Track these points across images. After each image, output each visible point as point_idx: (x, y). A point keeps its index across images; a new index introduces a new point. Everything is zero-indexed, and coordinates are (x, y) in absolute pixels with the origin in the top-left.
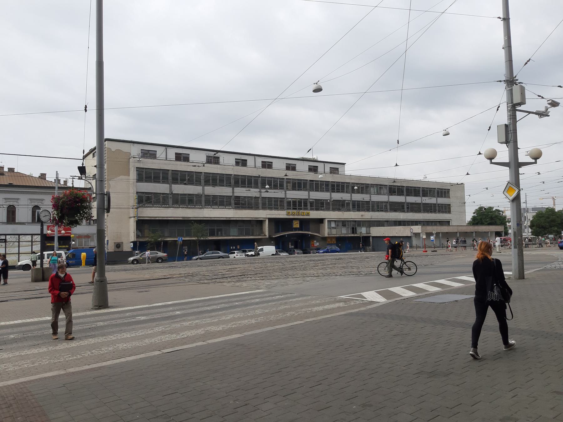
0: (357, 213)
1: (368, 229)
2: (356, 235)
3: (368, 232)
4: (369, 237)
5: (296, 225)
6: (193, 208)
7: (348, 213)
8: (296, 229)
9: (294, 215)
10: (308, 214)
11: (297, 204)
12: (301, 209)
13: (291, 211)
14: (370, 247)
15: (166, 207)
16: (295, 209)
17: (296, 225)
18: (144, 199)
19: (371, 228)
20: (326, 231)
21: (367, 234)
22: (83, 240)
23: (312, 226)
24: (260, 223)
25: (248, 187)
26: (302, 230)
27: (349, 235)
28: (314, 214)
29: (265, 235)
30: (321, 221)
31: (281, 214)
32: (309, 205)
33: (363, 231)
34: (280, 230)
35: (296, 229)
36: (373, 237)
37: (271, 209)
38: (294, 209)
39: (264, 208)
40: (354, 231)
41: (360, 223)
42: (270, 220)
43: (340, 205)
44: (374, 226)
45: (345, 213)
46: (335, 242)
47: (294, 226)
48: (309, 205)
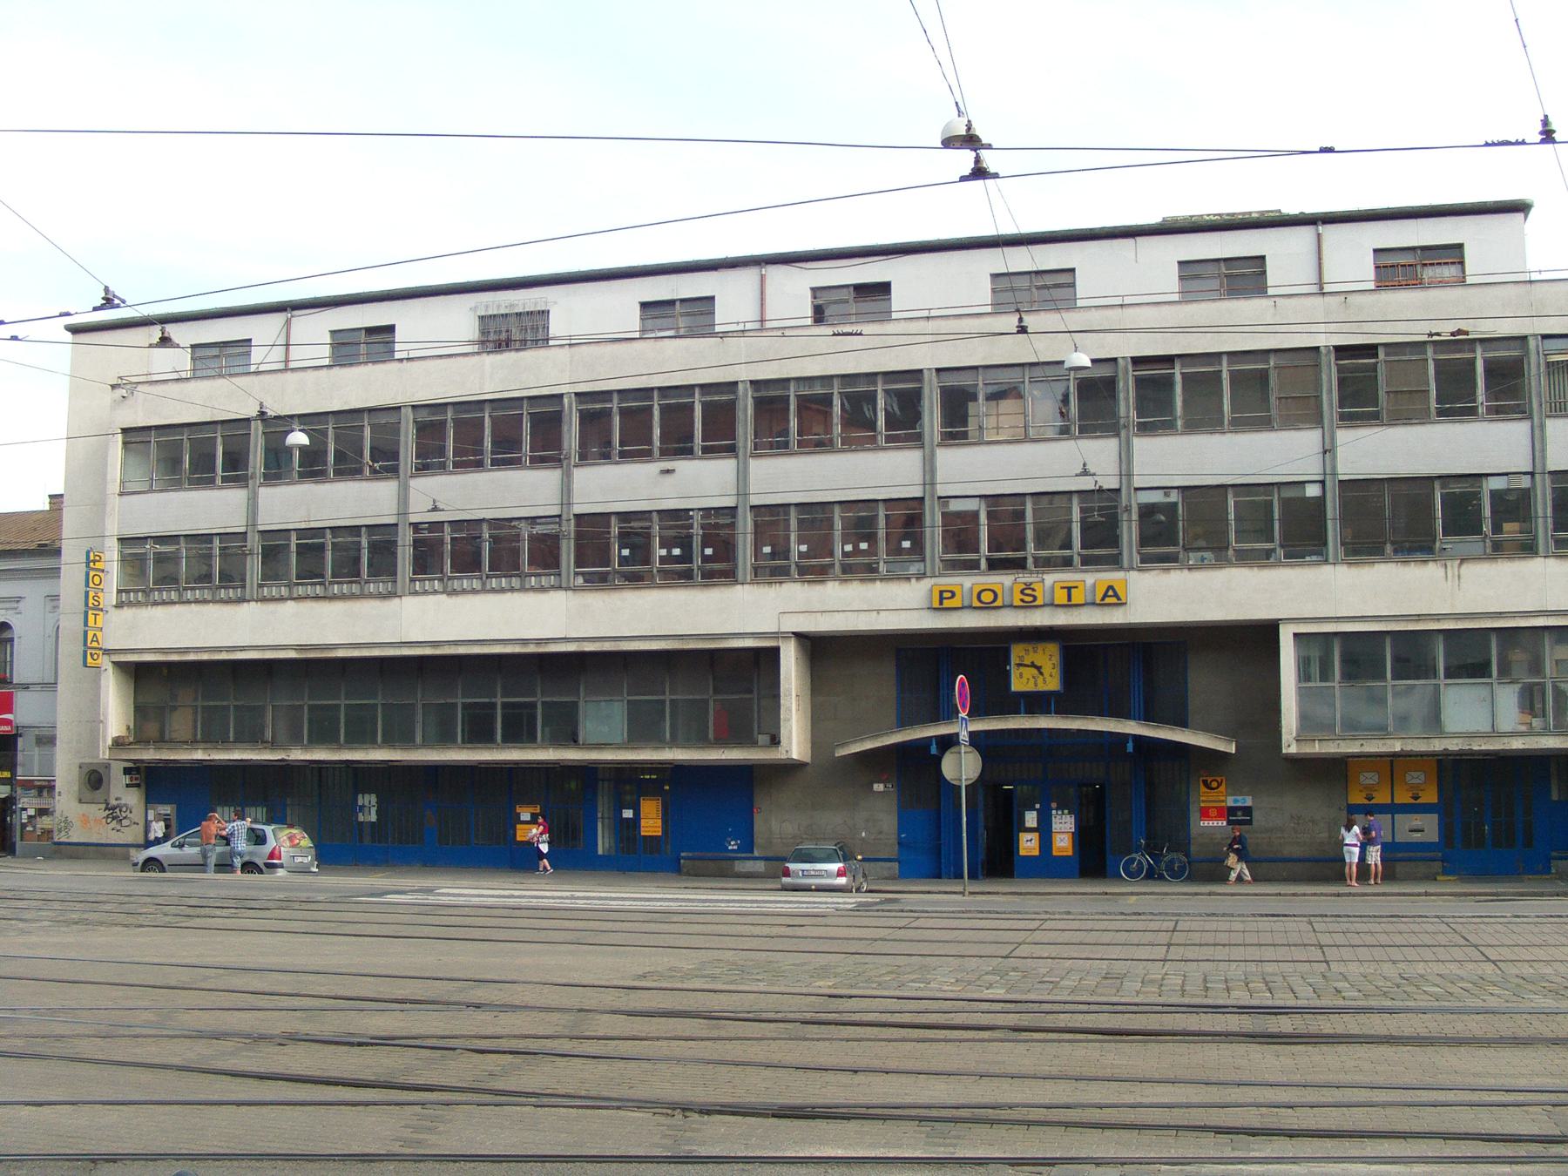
5: (1035, 672)
6: (352, 597)
8: (1036, 702)
10: (1112, 598)
11: (1006, 533)
12: (1067, 563)
13: (966, 583)
15: (228, 601)
16: (1019, 565)
17: (1035, 672)
18: (162, 567)
23: (1204, 682)
25: (666, 453)
28: (1161, 596)
29: (775, 741)
30: (1263, 635)
31: (894, 604)
32: (1129, 531)
35: (1036, 702)
37: (814, 572)
38: (994, 565)
39: (773, 570)
42: (822, 650)
43: (1399, 520)
45: (1473, 571)
46: (1430, 796)
47: (1017, 685)
48: (1129, 531)
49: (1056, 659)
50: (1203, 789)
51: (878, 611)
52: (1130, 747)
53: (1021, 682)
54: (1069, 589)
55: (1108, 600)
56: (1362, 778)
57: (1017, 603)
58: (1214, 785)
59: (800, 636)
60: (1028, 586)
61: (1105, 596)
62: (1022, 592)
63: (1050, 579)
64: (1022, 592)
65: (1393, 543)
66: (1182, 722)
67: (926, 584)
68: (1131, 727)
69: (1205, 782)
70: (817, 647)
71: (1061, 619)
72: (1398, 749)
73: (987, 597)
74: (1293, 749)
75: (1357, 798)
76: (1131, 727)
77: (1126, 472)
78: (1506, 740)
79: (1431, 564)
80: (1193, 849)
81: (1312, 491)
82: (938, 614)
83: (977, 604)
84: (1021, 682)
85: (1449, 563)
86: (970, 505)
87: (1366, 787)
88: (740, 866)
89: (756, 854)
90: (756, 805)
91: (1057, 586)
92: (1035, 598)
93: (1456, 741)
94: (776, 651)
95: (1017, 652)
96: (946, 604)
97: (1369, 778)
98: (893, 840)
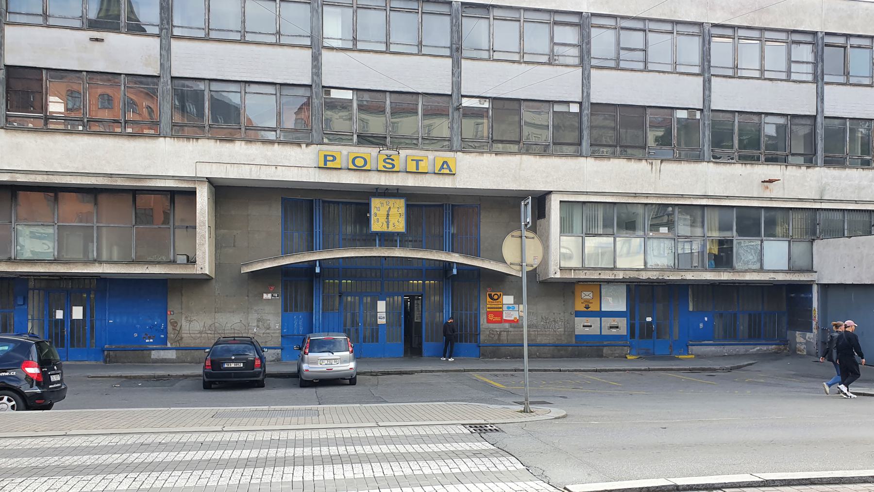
0: (739, 170)
1: (800, 248)
2: (725, 276)
3: (801, 263)
4: (806, 287)
5: (387, 216)
7: (686, 168)
8: (388, 239)
9: (358, 170)
14: (812, 336)
19: (817, 244)
20: (565, 251)
21: (791, 270)
22: (133, 256)
24: (172, 201)
26: (418, 245)
27: (689, 276)
33: (770, 259)
34: (318, 240)
36: (825, 288)
40: (723, 257)
41: (754, 221)
44: (838, 233)
49: (403, 210)
50: (489, 299)
51: (276, 167)
52: (455, 272)
53: (377, 225)
54: (417, 161)
55: (443, 171)
56: (583, 295)
57: (381, 168)
58: (496, 297)
59: (210, 181)
60: (389, 157)
61: (442, 168)
62: (384, 161)
63: (403, 153)
64: (384, 161)
65: (621, 147)
66: (476, 254)
67: (314, 148)
68: (456, 258)
69: (490, 296)
70: (223, 192)
71: (411, 181)
72: (621, 277)
73: (360, 162)
74: (558, 276)
75: (580, 307)
76: (456, 258)
77: (457, 84)
78: (683, 273)
79: (644, 161)
80: (482, 337)
81: (574, 109)
82: (321, 171)
83: (351, 166)
84: (377, 225)
85: (654, 162)
86: (348, 95)
87: (587, 301)
88: (155, 355)
89: (169, 345)
90: (170, 308)
91: (409, 159)
92: (394, 166)
93: (655, 273)
94: (192, 193)
95: (375, 203)
96: (329, 165)
97: (587, 295)
98: (278, 334)
